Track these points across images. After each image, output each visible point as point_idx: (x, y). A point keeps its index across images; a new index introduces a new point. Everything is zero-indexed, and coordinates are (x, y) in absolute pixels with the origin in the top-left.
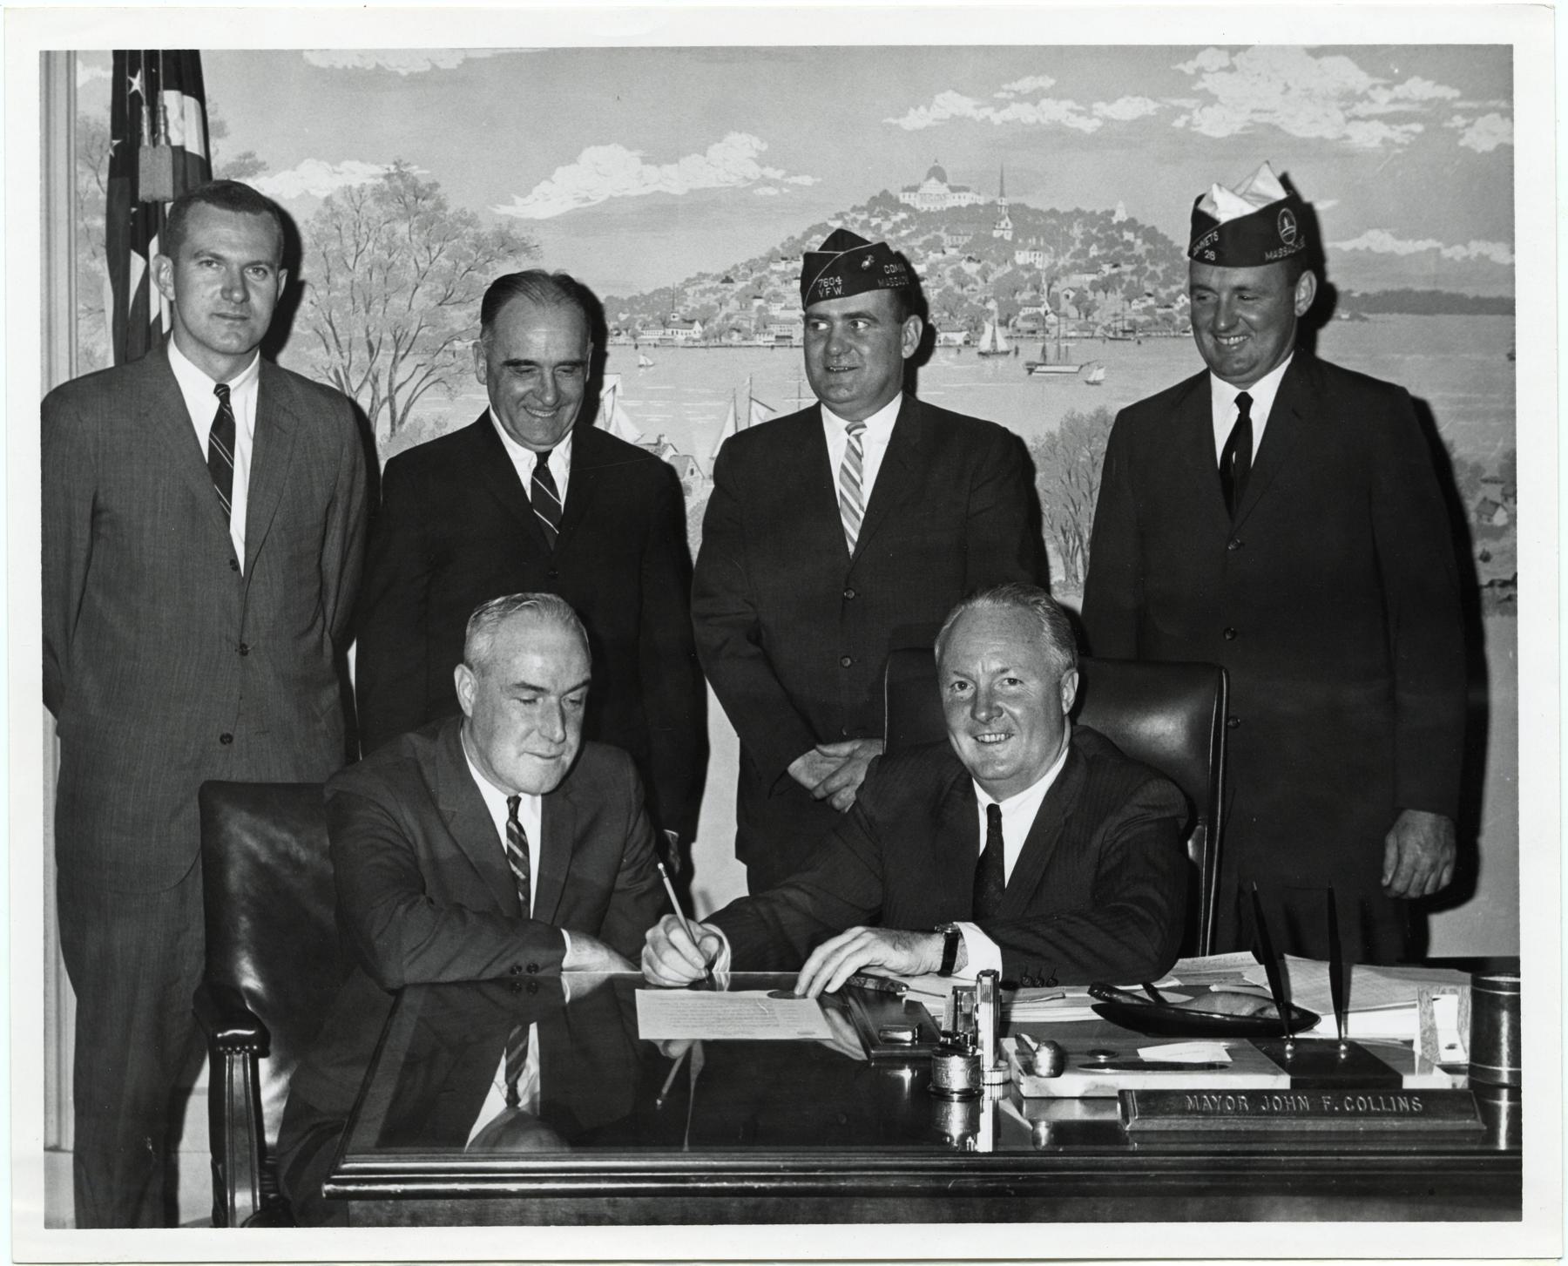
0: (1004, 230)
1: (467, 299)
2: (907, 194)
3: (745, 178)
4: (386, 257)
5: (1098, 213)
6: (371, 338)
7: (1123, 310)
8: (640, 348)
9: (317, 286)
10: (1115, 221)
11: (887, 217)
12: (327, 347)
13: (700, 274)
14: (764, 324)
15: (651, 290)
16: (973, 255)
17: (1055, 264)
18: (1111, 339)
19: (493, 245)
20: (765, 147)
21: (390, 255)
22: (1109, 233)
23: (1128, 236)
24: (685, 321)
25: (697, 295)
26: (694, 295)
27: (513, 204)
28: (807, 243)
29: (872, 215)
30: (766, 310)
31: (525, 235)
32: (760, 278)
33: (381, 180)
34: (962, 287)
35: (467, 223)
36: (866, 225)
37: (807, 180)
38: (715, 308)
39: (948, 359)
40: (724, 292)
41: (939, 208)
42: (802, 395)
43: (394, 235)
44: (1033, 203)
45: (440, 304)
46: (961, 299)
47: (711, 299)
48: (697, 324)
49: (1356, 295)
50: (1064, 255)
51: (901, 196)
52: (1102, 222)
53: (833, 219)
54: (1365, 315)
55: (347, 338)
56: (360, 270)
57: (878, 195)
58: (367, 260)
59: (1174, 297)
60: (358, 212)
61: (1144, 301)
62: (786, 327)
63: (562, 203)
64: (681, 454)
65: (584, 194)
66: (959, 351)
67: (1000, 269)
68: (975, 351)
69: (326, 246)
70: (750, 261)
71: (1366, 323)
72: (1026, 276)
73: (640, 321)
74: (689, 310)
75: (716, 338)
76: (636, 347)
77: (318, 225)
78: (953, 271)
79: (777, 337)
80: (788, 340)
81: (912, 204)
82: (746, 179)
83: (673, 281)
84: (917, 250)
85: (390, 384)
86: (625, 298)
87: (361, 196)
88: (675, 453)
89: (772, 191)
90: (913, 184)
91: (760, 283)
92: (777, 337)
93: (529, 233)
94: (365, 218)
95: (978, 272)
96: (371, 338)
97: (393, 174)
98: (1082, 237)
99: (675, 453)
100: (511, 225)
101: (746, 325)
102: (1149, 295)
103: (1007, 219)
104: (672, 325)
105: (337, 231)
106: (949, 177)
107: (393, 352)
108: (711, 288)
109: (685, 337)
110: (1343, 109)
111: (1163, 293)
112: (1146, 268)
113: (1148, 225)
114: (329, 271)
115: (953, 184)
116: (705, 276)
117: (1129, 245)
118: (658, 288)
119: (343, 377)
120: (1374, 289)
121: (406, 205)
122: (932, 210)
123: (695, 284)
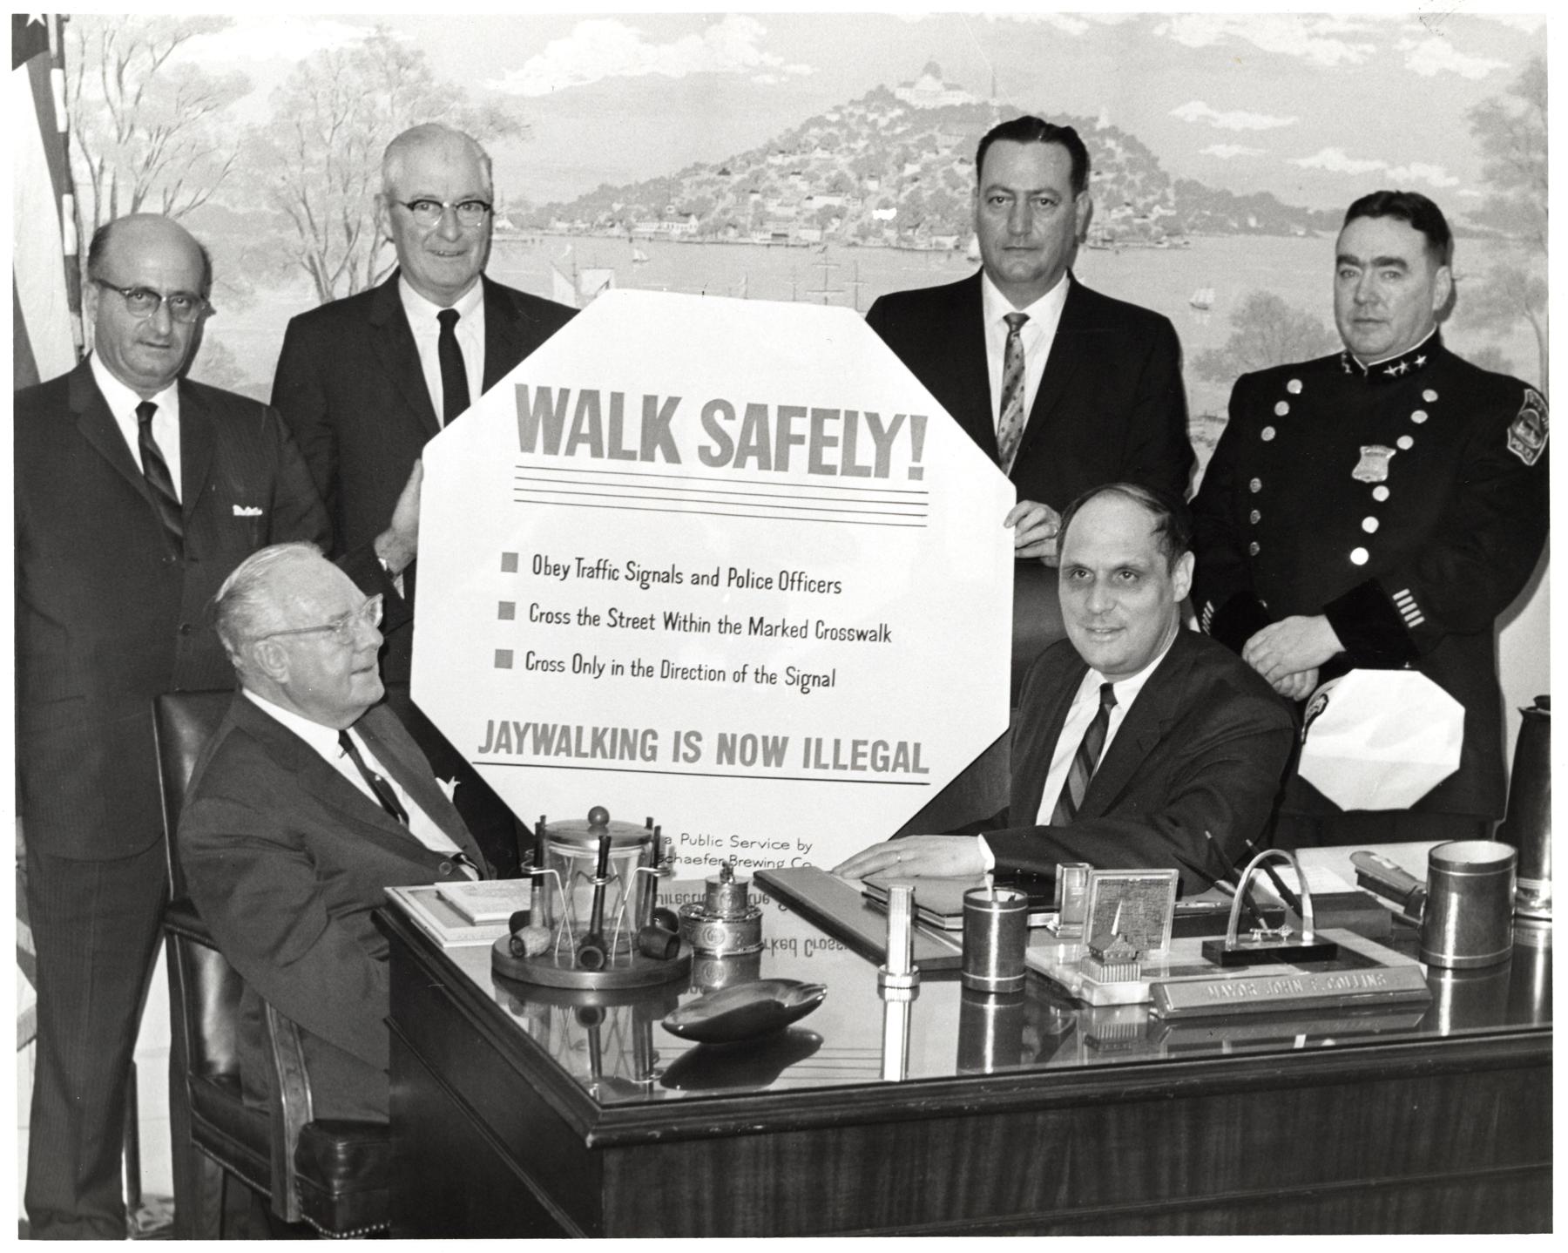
2: (903, 90)
4: (366, 130)
6: (349, 220)
7: (1104, 219)
8: (635, 243)
9: (290, 160)
10: (1098, 126)
11: (883, 114)
12: (301, 230)
18: (1092, 248)
20: (764, 31)
21: (371, 129)
22: (1093, 139)
23: (1110, 143)
25: (694, 187)
26: (691, 187)
28: (805, 136)
30: (763, 206)
33: (360, 45)
35: (454, 97)
36: (863, 118)
37: (805, 69)
38: (710, 201)
39: (939, 264)
40: (721, 185)
41: (933, 106)
42: (797, 296)
43: (374, 106)
46: (954, 202)
47: (708, 192)
49: (1310, 212)
53: (830, 112)
54: (1319, 232)
55: (323, 219)
56: (337, 146)
57: (873, 87)
58: (346, 134)
59: (1149, 207)
60: (335, 79)
61: (1123, 210)
62: (783, 225)
66: (949, 256)
68: (964, 256)
69: (300, 115)
70: (747, 153)
73: (633, 213)
74: (686, 202)
75: (714, 232)
76: (631, 240)
77: (291, 92)
78: (944, 172)
80: (782, 241)
81: (908, 100)
83: (666, 168)
84: (911, 148)
85: (370, 273)
86: (619, 184)
87: (339, 61)
89: (770, 79)
90: (912, 80)
91: (757, 177)
92: (774, 235)
94: (343, 86)
96: (349, 220)
97: (375, 39)
101: (742, 220)
102: (1128, 204)
105: (312, 100)
107: (373, 237)
109: (679, 232)
110: (1305, 26)
111: (1140, 202)
112: (1124, 178)
113: (1129, 133)
114: (303, 144)
117: (1111, 153)
118: (653, 177)
119: (318, 265)
121: (388, 74)
122: (927, 108)
123: (690, 175)
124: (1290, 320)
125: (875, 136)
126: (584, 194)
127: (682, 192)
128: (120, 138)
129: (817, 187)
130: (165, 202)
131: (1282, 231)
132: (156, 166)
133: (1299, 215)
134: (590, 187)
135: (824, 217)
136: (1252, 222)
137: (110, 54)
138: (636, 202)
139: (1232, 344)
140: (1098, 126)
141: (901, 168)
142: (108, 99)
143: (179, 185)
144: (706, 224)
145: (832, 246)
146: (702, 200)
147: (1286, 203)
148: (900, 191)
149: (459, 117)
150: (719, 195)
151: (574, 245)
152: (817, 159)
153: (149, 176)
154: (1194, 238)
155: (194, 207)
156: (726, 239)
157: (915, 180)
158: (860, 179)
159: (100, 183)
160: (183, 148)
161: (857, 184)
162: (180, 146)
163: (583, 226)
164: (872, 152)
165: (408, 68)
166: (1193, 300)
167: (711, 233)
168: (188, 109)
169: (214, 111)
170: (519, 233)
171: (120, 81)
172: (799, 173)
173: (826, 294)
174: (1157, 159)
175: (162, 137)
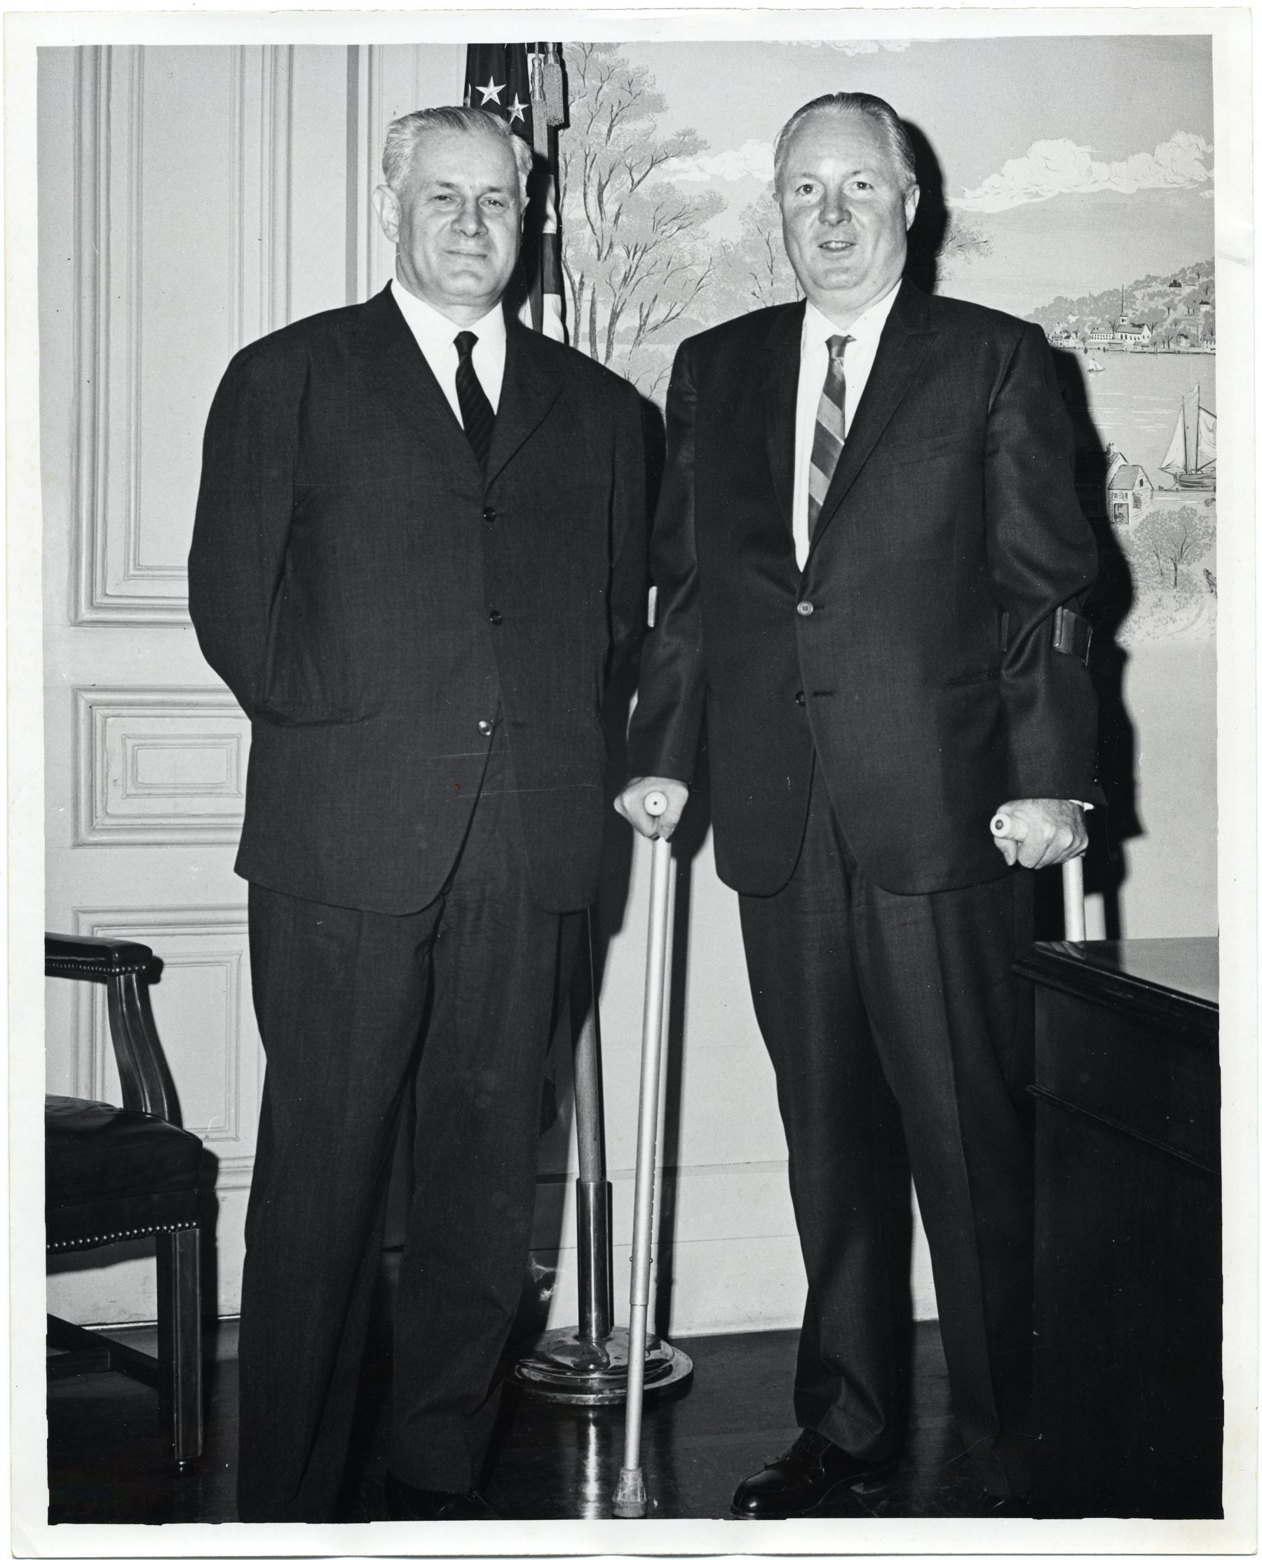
3: (1191, 180)
13: (1148, 276)
15: (1100, 292)
24: (1134, 325)
25: (1146, 298)
26: (1143, 299)
27: (963, 197)
31: (974, 229)
32: (1207, 282)
40: (1171, 296)
47: (1160, 303)
48: (1146, 326)
64: (1131, 463)
70: (1197, 264)
73: (1088, 324)
74: (1138, 313)
77: (761, 211)
86: (1075, 299)
88: (1125, 463)
93: (979, 228)
99: (1125, 463)
104: (1122, 329)
108: (1160, 291)
109: (1133, 341)
114: (772, 261)
116: (1155, 278)
118: (1106, 289)
123: (1142, 288)
126: (1040, 307)
127: (1135, 303)
128: (599, 256)
130: (641, 317)
132: (633, 282)
137: (591, 175)
138: (1091, 314)
142: (588, 217)
143: (654, 301)
144: (1159, 334)
146: (1154, 312)
153: (626, 292)
155: (669, 321)
156: (1178, 348)
159: (579, 299)
160: (659, 263)
162: (656, 262)
167: (1164, 343)
168: (664, 228)
169: (688, 228)
171: (600, 202)
175: (639, 254)
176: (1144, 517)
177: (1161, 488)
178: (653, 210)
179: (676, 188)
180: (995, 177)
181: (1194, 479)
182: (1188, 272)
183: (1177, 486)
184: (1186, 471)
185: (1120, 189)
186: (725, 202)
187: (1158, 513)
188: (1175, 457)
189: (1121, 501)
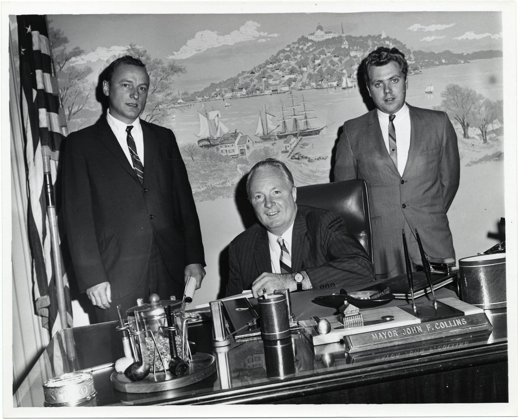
0: (345, 45)
1: (162, 90)
2: (310, 36)
5: (376, 36)
10: (382, 38)
11: (305, 45)
14: (267, 86)
15: (226, 79)
16: (336, 55)
17: (364, 55)
19: (169, 70)
20: (259, 25)
22: (381, 42)
24: (240, 89)
27: (174, 54)
28: (278, 57)
29: (300, 45)
30: (268, 82)
31: (179, 65)
32: (263, 71)
33: (126, 52)
34: (334, 66)
36: (298, 48)
37: (276, 35)
38: (249, 83)
41: (322, 40)
42: (284, 109)
44: (354, 34)
45: (152, 93)
46: (335, 70)
47: (248, 80)
49: (465, 54)
50: (366, 51)
51: (308, 37)
52: (378, 39)
54: (469, 61)
62: (275, 87)
63: (191, 52)
64: (244, 135)
65: (198, 49)
66: (335, 88)
67: (346, 59)
68: (341, 88)
70: (260, 65)
71: (469, 64)
72: (355, 60)
76: (224, 100)
78: (330, 61)
79: (272, 91)
80: (276, 91)
81: (313, 39)
82: (254, 37)
83: (234, 75)
84: (316, 55)
86: (217, 82)
89: (264, 40)
90: (313, 32)
92: (272, 91)
95: (338, 60)
98: (372, 44)
100: (174, 62)
101: (261, 88)
103: (346, 41)
106: (324, 29)
109: (240, 94)
113: (393, 38)
115: (326, 31)
116: (245, 72)
118: (229, 78)
120: (470, 52)
122: (320, 41)
124: (463, 92)
125: (303, 53)
126: (206, 87)
127: (239, 81)
129: (286, 73)
131: (456, 63)
132: (65, 100)
133: (461, 56)
134: (208, 85)
135: (289, 82)
136: (444, 61)
138: (224, 87)
139: (443, 104)
140: (382, 38)
141: (314, 62)
143: (73, 105)
144: (248, 90)
145: (293, 91)
147: (455, 53)
148: (315, 70)
149: (161, 69)
150: (252, 81)
151: (205, 104)
152: (284, 63)
154: (423, 70)
156: (256, 94)
157: (320, 65)
158: (300, 67)
161: (299, 70)
162: (72, 92)
163: (207, 98)
164: (303, 58)
165: (142, 57)
166: (426, 91)
168: (73, 81)
170: (185, 103)
172: (278, 69)
173: (293, 107)
174: (405, 45)
175: (65, 91)
176: (251, 152)
177: (256, 142)
178: (68, 75)
179: (76, 67)
180: (184, 47)
181: (267, 137)
182: (256, 68)
183: (262, 140)
184: (264, 134)
185: (228, 44)
186: (92, 69)
187: (256, 150)
188: (260, 131)
189: (242, 148)
